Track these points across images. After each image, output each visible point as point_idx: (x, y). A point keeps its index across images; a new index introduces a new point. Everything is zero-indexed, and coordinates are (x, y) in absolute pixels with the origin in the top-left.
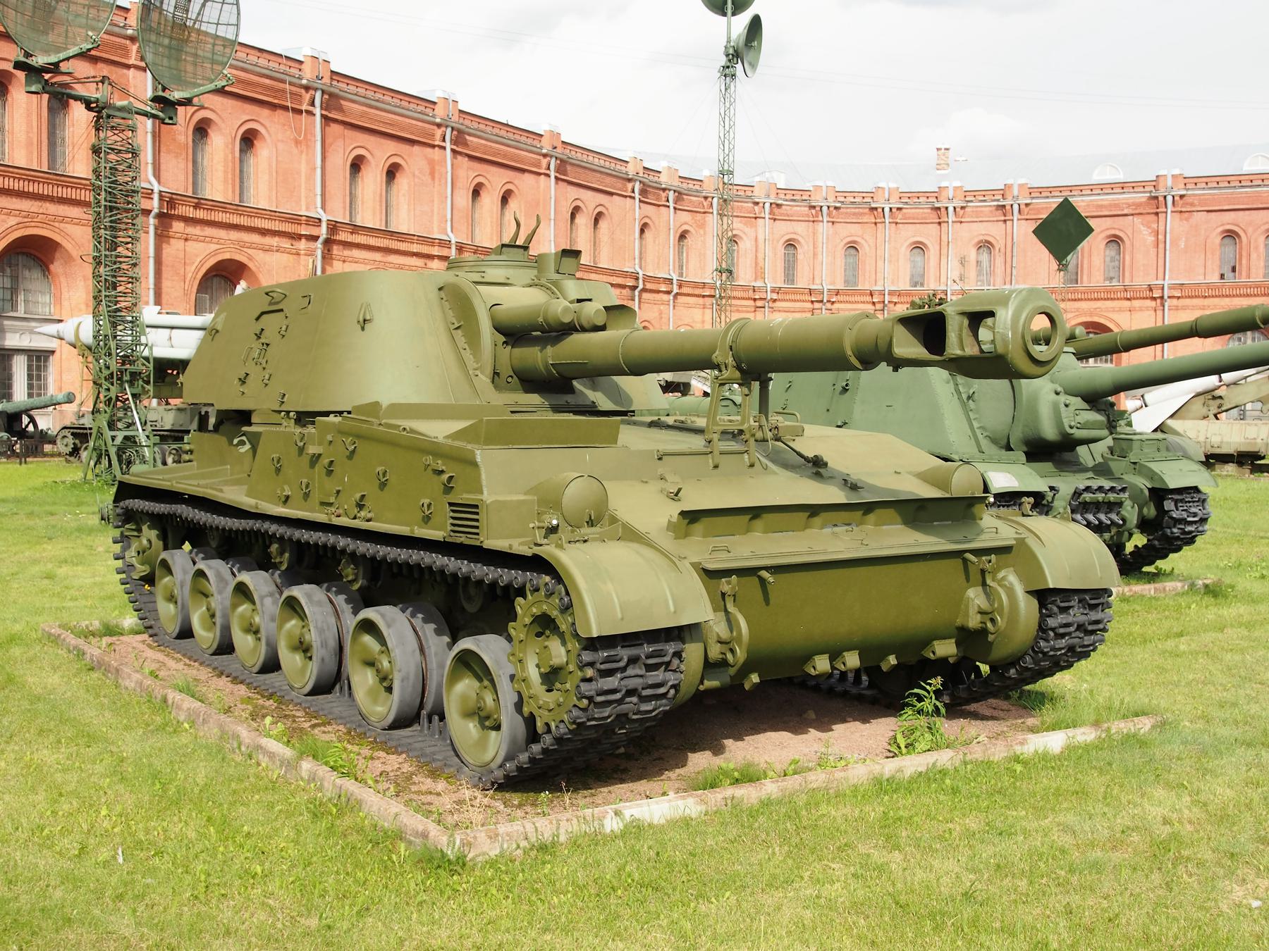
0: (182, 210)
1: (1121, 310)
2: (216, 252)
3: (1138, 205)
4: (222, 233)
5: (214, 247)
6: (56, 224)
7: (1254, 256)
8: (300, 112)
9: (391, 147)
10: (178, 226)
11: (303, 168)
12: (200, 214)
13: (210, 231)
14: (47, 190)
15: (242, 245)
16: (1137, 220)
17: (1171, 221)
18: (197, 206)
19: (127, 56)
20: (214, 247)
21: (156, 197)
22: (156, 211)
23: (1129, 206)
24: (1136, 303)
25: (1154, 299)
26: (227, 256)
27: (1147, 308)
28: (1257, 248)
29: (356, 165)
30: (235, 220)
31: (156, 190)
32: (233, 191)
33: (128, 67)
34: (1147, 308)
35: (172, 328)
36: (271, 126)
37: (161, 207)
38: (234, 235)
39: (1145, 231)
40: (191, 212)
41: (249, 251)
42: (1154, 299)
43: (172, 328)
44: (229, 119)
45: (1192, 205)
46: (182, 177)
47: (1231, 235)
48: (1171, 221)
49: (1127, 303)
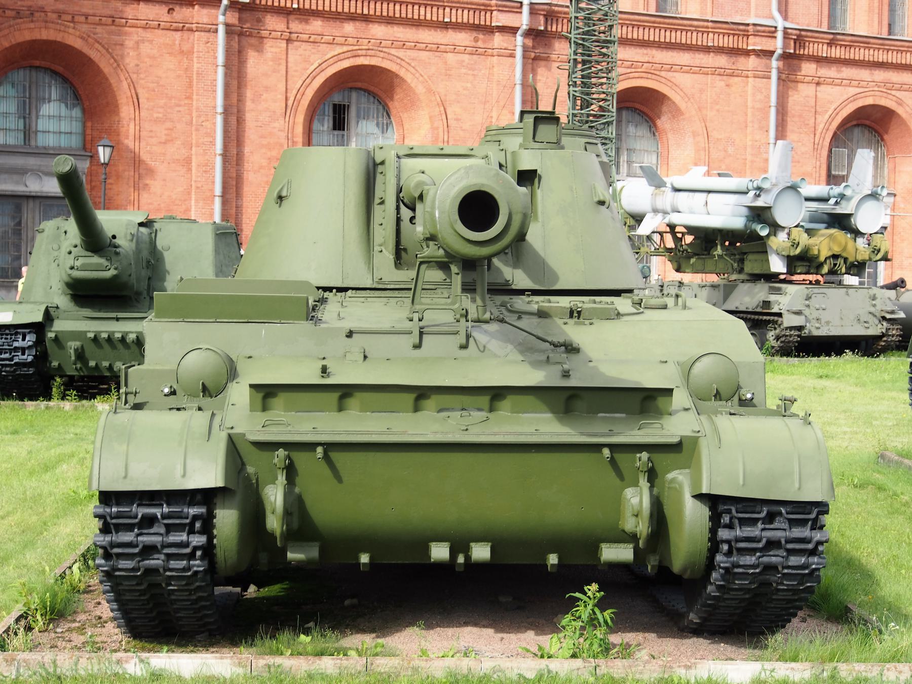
0: (811, 49)
2: (855, 97)
4: (864, 74)
5: (852, 91)
6: (663, 74)
10: (808, 68)
12: (836, 52)
13: (848, 72)
14: (652, 35)
15: (889, 86)
18: (830, 44)
20: (852, 91)
21: (780, 35)
22: (779, 51)
26: (870, 101)
30: (881, 57)
31: (780, 28)
32: (880, 23)
35: (709, 192)
37: (785, 46)
38: (880, 75)
40: (824, 51)
41: (898, 94)
43: (709, 192)
46: (815, 10)
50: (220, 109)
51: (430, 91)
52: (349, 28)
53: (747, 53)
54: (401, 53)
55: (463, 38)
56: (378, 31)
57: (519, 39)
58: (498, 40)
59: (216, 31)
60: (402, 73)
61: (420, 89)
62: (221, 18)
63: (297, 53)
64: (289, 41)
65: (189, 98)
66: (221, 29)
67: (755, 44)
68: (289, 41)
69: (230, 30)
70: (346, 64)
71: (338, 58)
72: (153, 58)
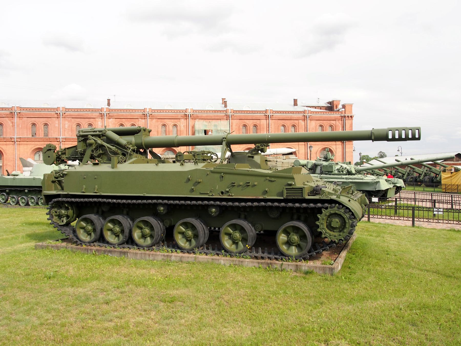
1: (3, 145)
3: (7, 114)
7: (40, 130)
16: (7, 118)
17: (16, 120)
23: (4, 114)
24: (8, 143)
25: (13, 142)
27: (11, 144)
28: (41, 128)
34: (11, 144)
39: (10, 122)
42: (13, 142)
45: (23, 115)
47: (34, 124)
48: (16, 120)
49: (5, 143)
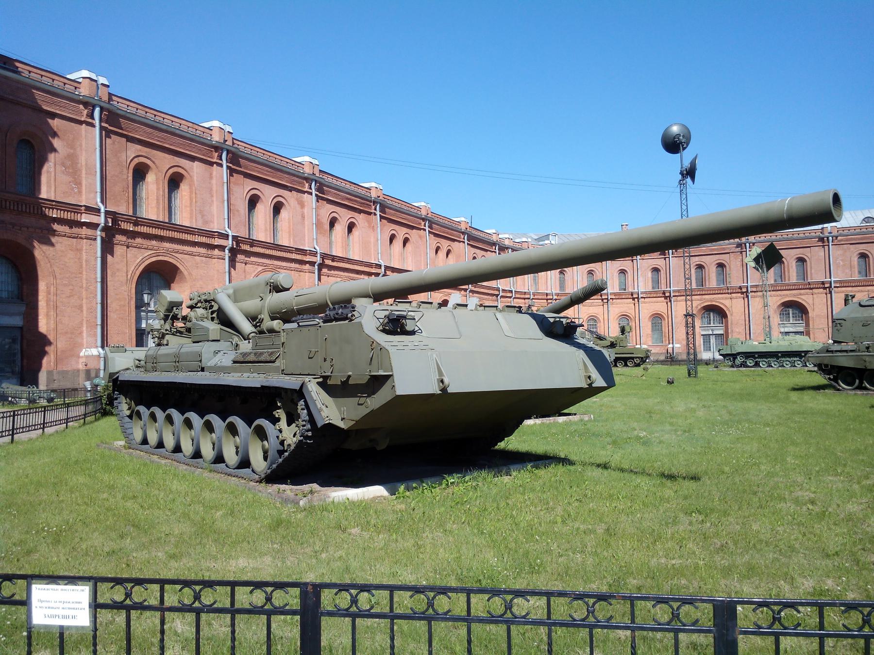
8: (370, 214)
9: (405, 230)
11: (372, 240)
19: (304, 186)
29: (392, 238)
33: (304, 192)
36: (360, 220)
44: (345, 217)
50: (99, 280)
51: (190, 274)
52: (154, 242)
53: (305, 263)
54: (177, 255)
55: (203, 250)
56: (167, 245)
57: (227, 251)
58: (216, 252)
59: (95, 239)
60: (178, 265)
61: (185, 273)
62: (99, 233)
63: (132, 252)
64: (128, 247)
65: (81, 273)
66: (99, 239)
67: (308, 258)
68: (128, 247)
69: (103, 240)
70: (154, 259)
71: (150, 256)
72: (62, 251)
